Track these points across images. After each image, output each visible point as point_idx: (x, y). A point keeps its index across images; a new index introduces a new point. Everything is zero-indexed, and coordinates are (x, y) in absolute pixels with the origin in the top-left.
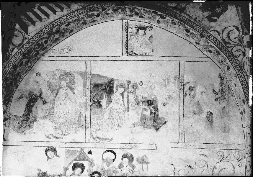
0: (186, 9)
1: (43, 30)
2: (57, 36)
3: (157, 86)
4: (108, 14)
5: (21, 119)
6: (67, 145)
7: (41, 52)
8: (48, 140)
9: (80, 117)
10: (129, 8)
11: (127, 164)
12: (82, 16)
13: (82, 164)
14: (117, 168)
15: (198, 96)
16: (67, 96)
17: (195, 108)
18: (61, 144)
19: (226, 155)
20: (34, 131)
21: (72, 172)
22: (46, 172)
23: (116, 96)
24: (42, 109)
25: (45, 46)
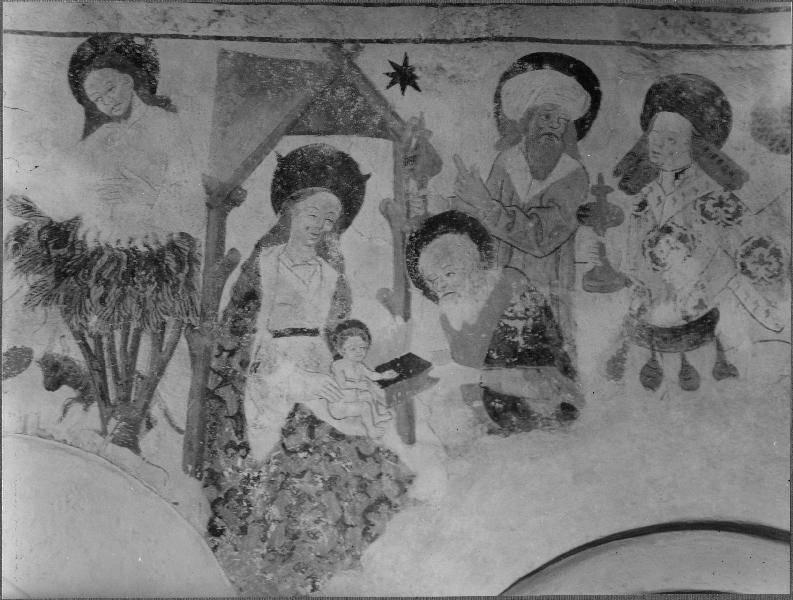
11: (684, 160)
14: (609, 190)
21: (271, 219)
22: (76, 221)
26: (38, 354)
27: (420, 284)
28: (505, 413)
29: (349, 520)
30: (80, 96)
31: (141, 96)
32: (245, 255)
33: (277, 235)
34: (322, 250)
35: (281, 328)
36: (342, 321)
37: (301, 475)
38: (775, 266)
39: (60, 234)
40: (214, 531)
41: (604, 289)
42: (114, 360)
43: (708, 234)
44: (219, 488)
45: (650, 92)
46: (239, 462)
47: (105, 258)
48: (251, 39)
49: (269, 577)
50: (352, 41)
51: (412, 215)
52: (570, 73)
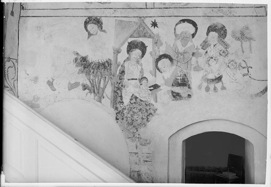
6: (118, 14)
11: (216, 42)
21: (127, 56)
26: (81, 83)
27: (158, 69)
28: (176, 96)
29: (144, 117)
30: (87, 31)
31: (99, 30)
32: (122, 63)
33: (128, 59)
34: (138, 62)
35: (129, 78)
36: (142, 77)
37: (134, 108)
38: (236, 66)
39: (84, 59)
40: (117, 119)
41: (198, 71)
42: (96, 85)
43: (221, 59)
44: (118, 110)
45: (209, 27)
46: (121, 105)
47: (93, 64)
48: (122, 17)
49: (128, 128)
50: (143, 17)
51: (156, 55)
52: (191, 23)
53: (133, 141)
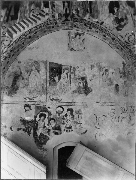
0: (103, 23)
1: (21, 37)
2: (30, 40)
3: (87, 69)
4: (58, 26)
5: (10, 88)
7: (21, 49)
8: (25, 100)
9: (43, 87)
10: (71, 23)
12: (43, 28)
13: (45, 114)
15: (110, 75)
16: (36, 75)
17: (109, 82)
18: (33, 103)
19: (126, 110)
20: (18, 95)
23: (63, 75)
24: (22, 83)
25: (23, 45)
27: (50, 123)
28: (56, 134)
30: (25, 109)
33: (40, 120)
53: (41, 150)
